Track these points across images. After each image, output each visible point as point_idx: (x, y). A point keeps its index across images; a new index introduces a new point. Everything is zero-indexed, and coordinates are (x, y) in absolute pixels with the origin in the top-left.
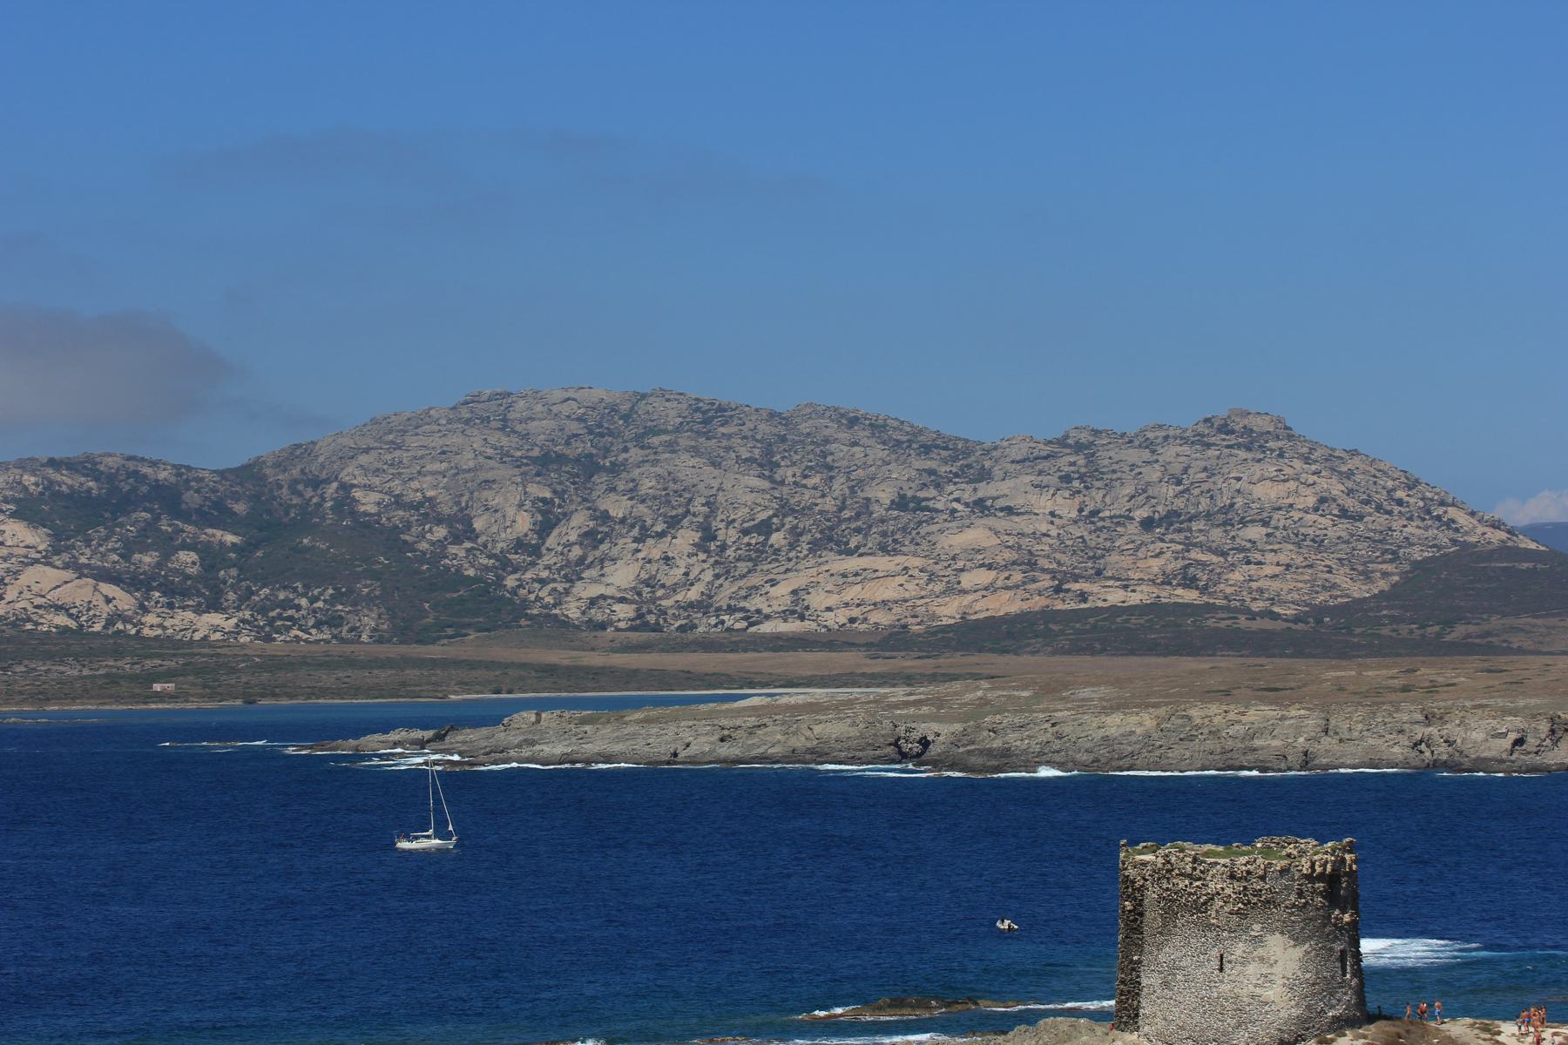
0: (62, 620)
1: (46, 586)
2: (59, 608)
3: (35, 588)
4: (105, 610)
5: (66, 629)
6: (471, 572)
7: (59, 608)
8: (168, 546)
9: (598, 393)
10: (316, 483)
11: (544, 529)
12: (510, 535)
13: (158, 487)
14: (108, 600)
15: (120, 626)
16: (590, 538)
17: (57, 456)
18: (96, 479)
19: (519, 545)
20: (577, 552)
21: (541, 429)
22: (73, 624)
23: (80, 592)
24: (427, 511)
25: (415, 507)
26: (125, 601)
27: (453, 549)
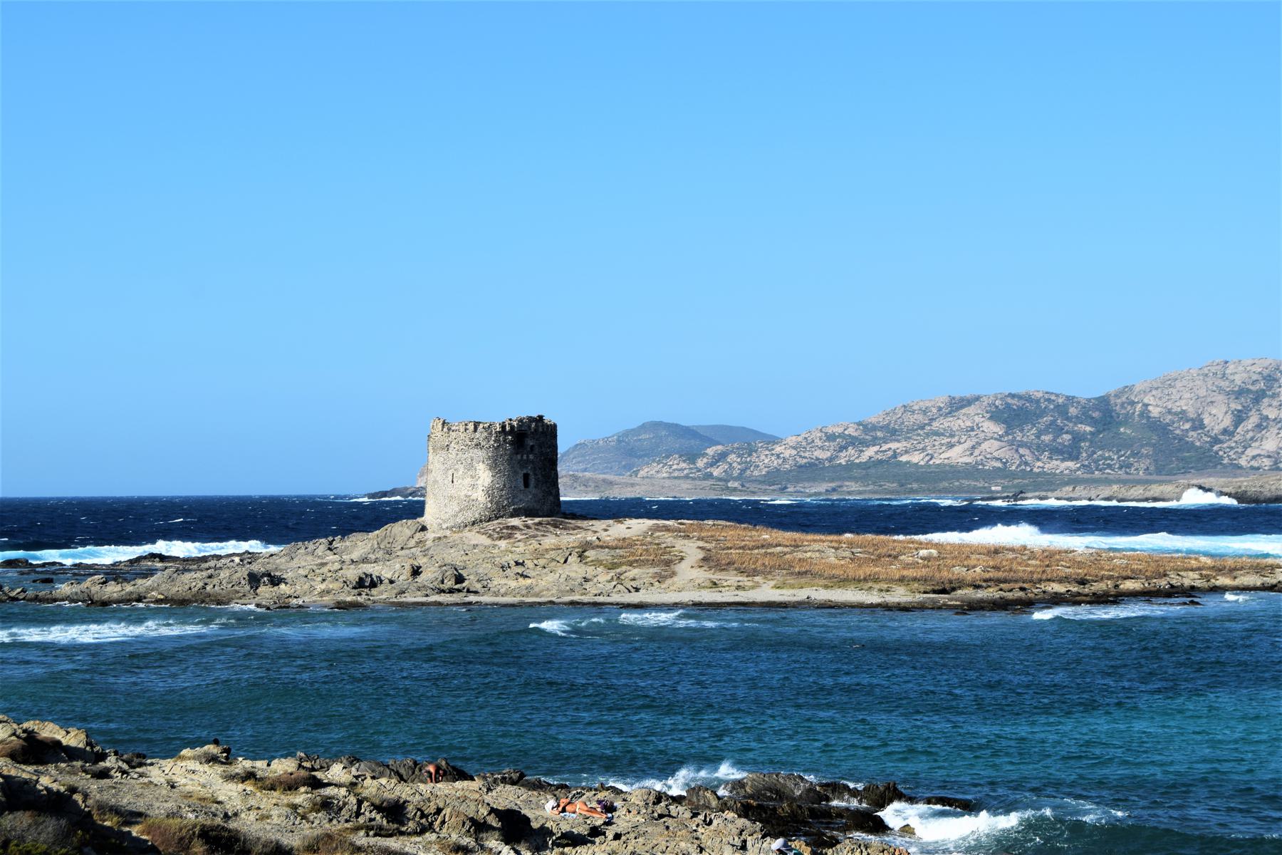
0: (998, 465)
1: (992, 450)
6: (1198, 444)
8: (1060, 430)
9: (1266, 363)
10: (1133, 403)
12: (1222, 426)
13: (1058, 406)
16: (1259, 427)
19: (1225, 431)
20: (1251, 434)
21: (1238, 379)
24: (1182, 415)
25: (1176, 414)
27: (1191, 433)
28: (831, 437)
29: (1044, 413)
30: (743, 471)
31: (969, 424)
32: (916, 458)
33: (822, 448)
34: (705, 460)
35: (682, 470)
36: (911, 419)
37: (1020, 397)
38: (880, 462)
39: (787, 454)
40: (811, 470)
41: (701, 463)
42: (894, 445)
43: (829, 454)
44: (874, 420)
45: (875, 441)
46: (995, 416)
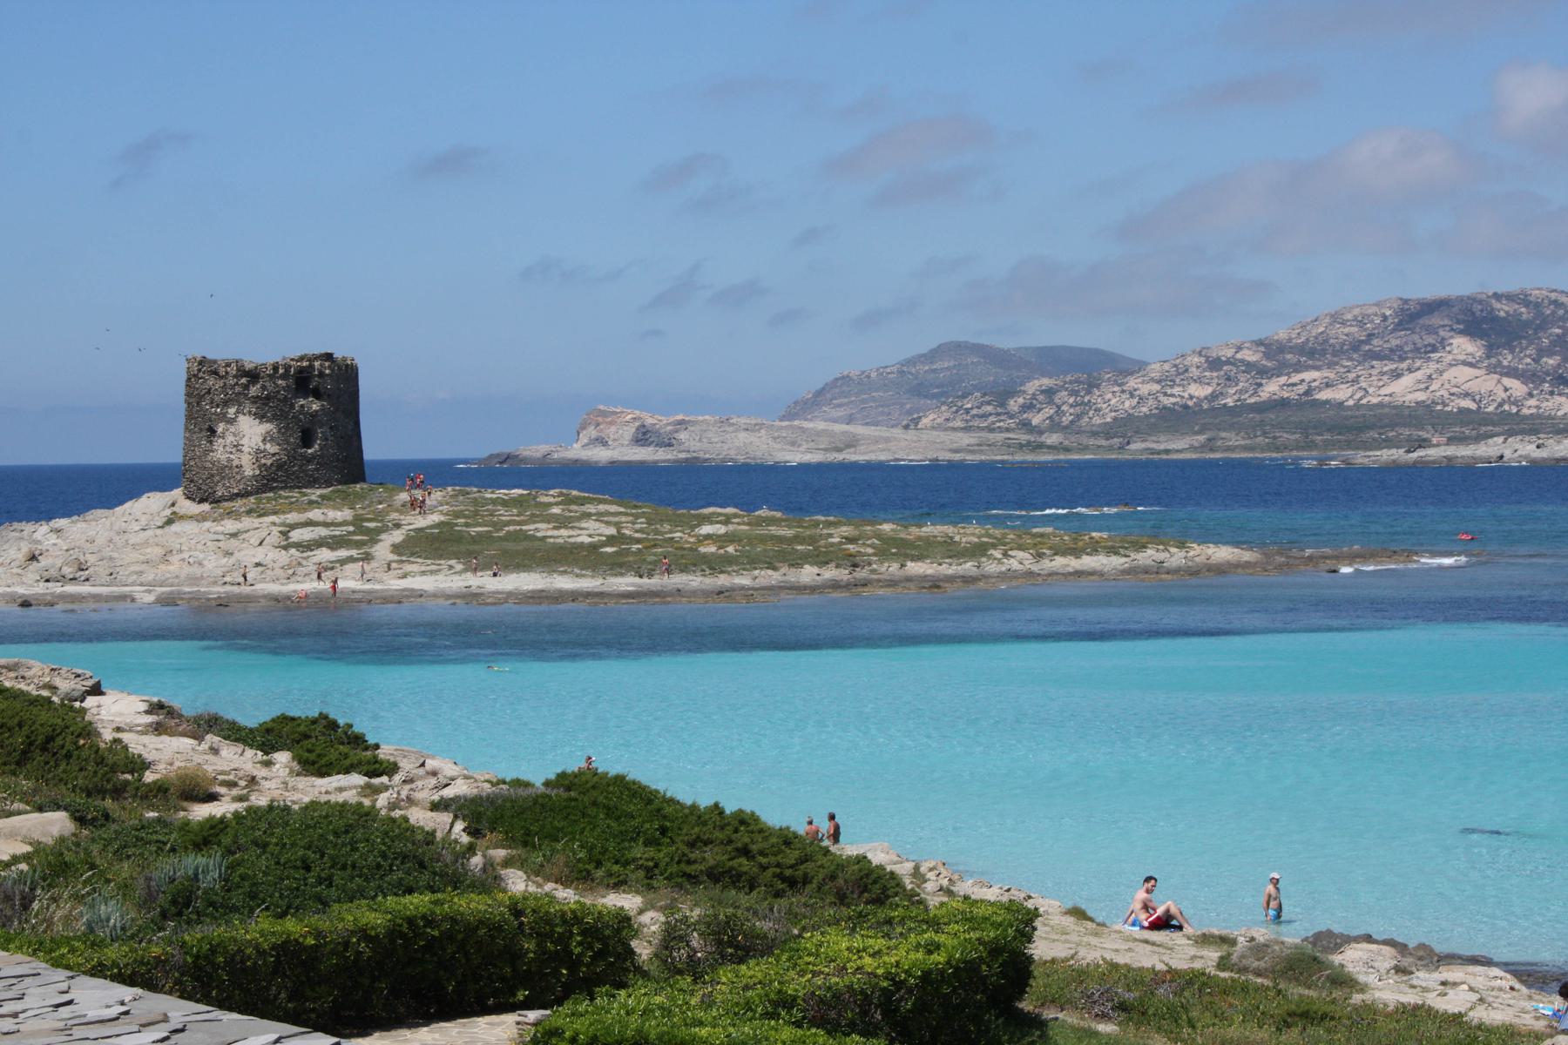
1: (1461, 380)
2: (1466, 395)
3: (1454, 382)
4: (1502, 395)
5: (1468, 410)
7: (1466, 395)
14: (1506, 390)
15: (1506, 407)
17: (1499, 291)
18: (1527, 306)
22: (1473, 406)
26: (1517, 387)
28: (1215, 364)
29: (1542, 324)
30: (1079, 417)
31: (1430, 340)
32: (1341, 393)
33: (1199, 381)
34: (1021, 400)
35: (985, 416)
36: (1341, 333)
37: (1510, 298)
38: (1283, 403)
39: (1145, 389)
40: (1176, 418)
41: (1014, 404)
42: (1315, 374)
43: (1209, 390)
44: (1282, 335)
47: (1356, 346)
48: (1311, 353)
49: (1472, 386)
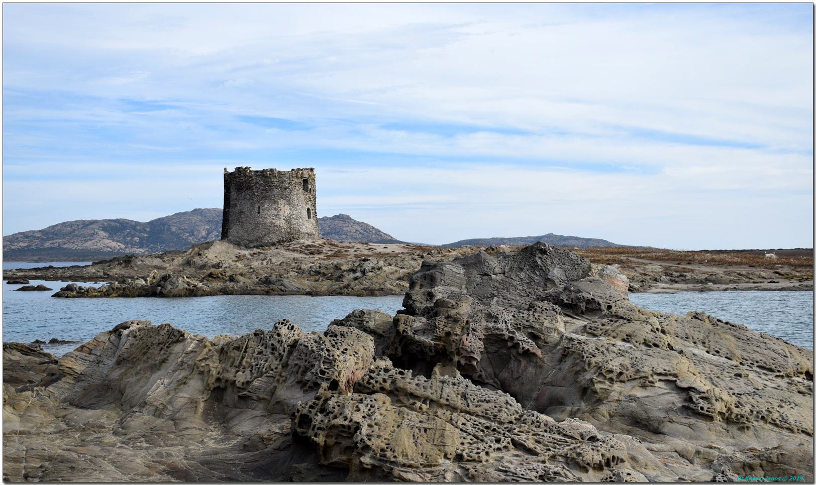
8: (133, 236)
10: (164, 225)
11: (208, 234)
23: (114, 244)
24: (185, 230)
26: (123, 246)
38: (51, 248)
45: (48, 239)
46: (104, 229)
47: (70, 233)
48: (56, 235)
49: (110, 245)
